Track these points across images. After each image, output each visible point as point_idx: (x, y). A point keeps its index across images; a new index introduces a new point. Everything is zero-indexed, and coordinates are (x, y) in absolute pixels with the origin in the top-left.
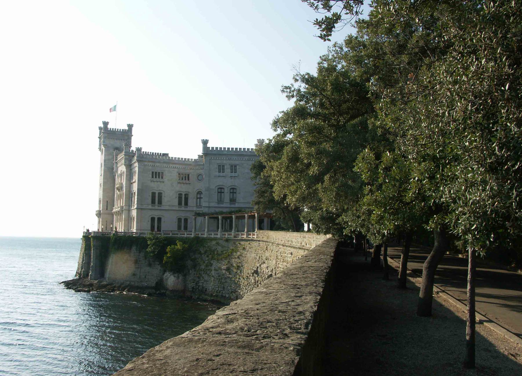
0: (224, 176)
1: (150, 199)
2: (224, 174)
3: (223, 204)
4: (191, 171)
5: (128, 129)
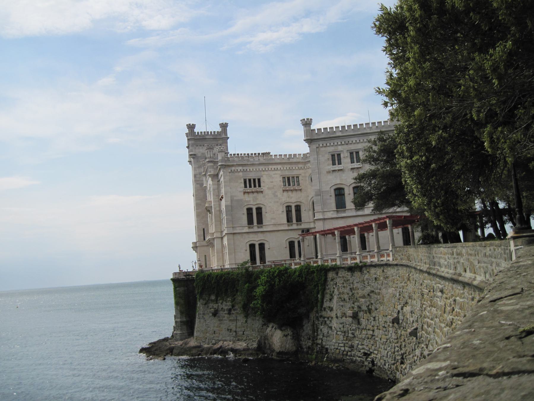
0: (341, 170)
4: (301, 172)
5: (222, 130)
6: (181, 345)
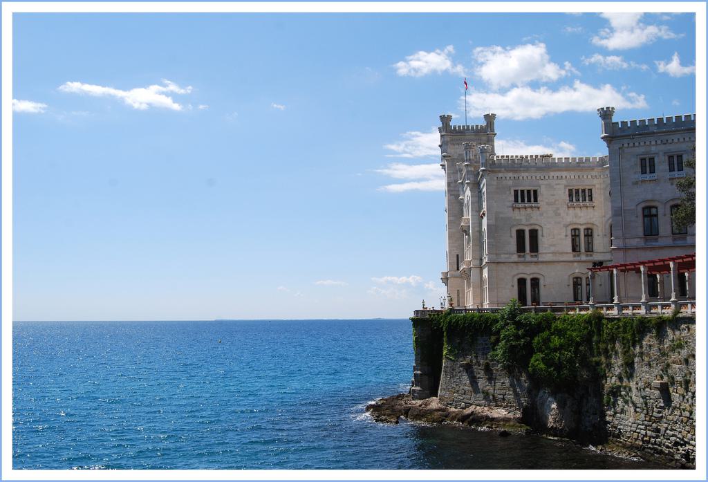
3: (656, 240)
4: (595, 181)
5: (487, 123)
6: (420, 406)
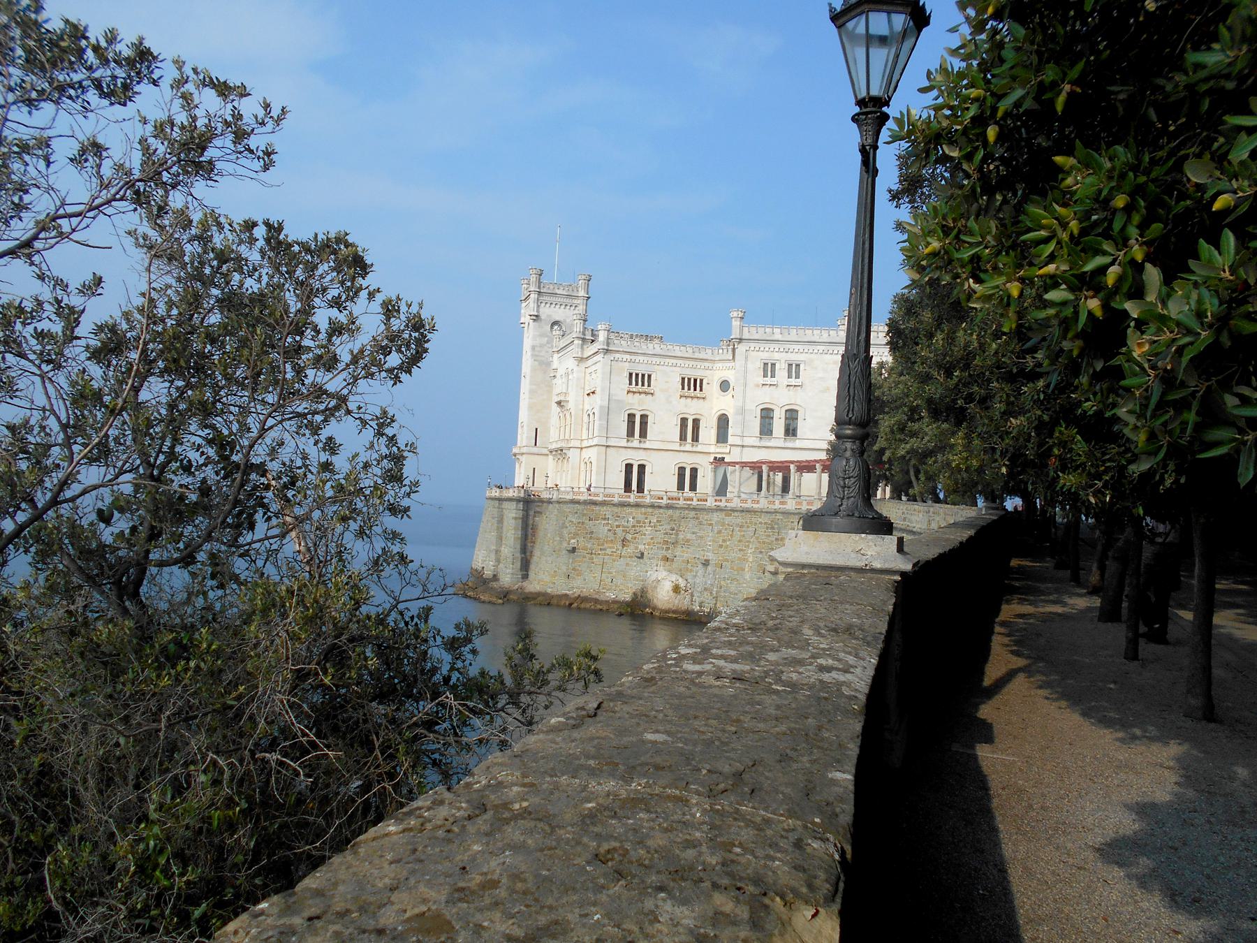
1: (625, 426)
2: (774, 381)
4: (708, 372)
